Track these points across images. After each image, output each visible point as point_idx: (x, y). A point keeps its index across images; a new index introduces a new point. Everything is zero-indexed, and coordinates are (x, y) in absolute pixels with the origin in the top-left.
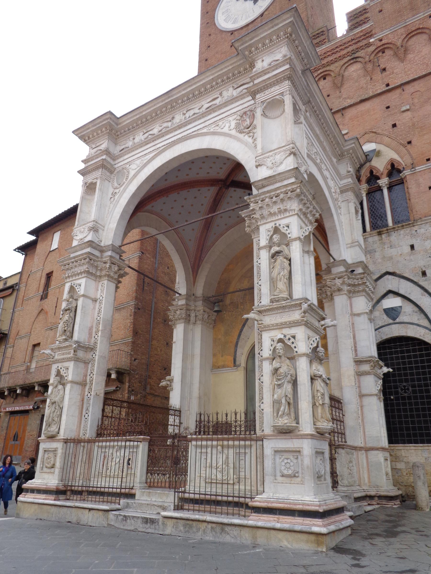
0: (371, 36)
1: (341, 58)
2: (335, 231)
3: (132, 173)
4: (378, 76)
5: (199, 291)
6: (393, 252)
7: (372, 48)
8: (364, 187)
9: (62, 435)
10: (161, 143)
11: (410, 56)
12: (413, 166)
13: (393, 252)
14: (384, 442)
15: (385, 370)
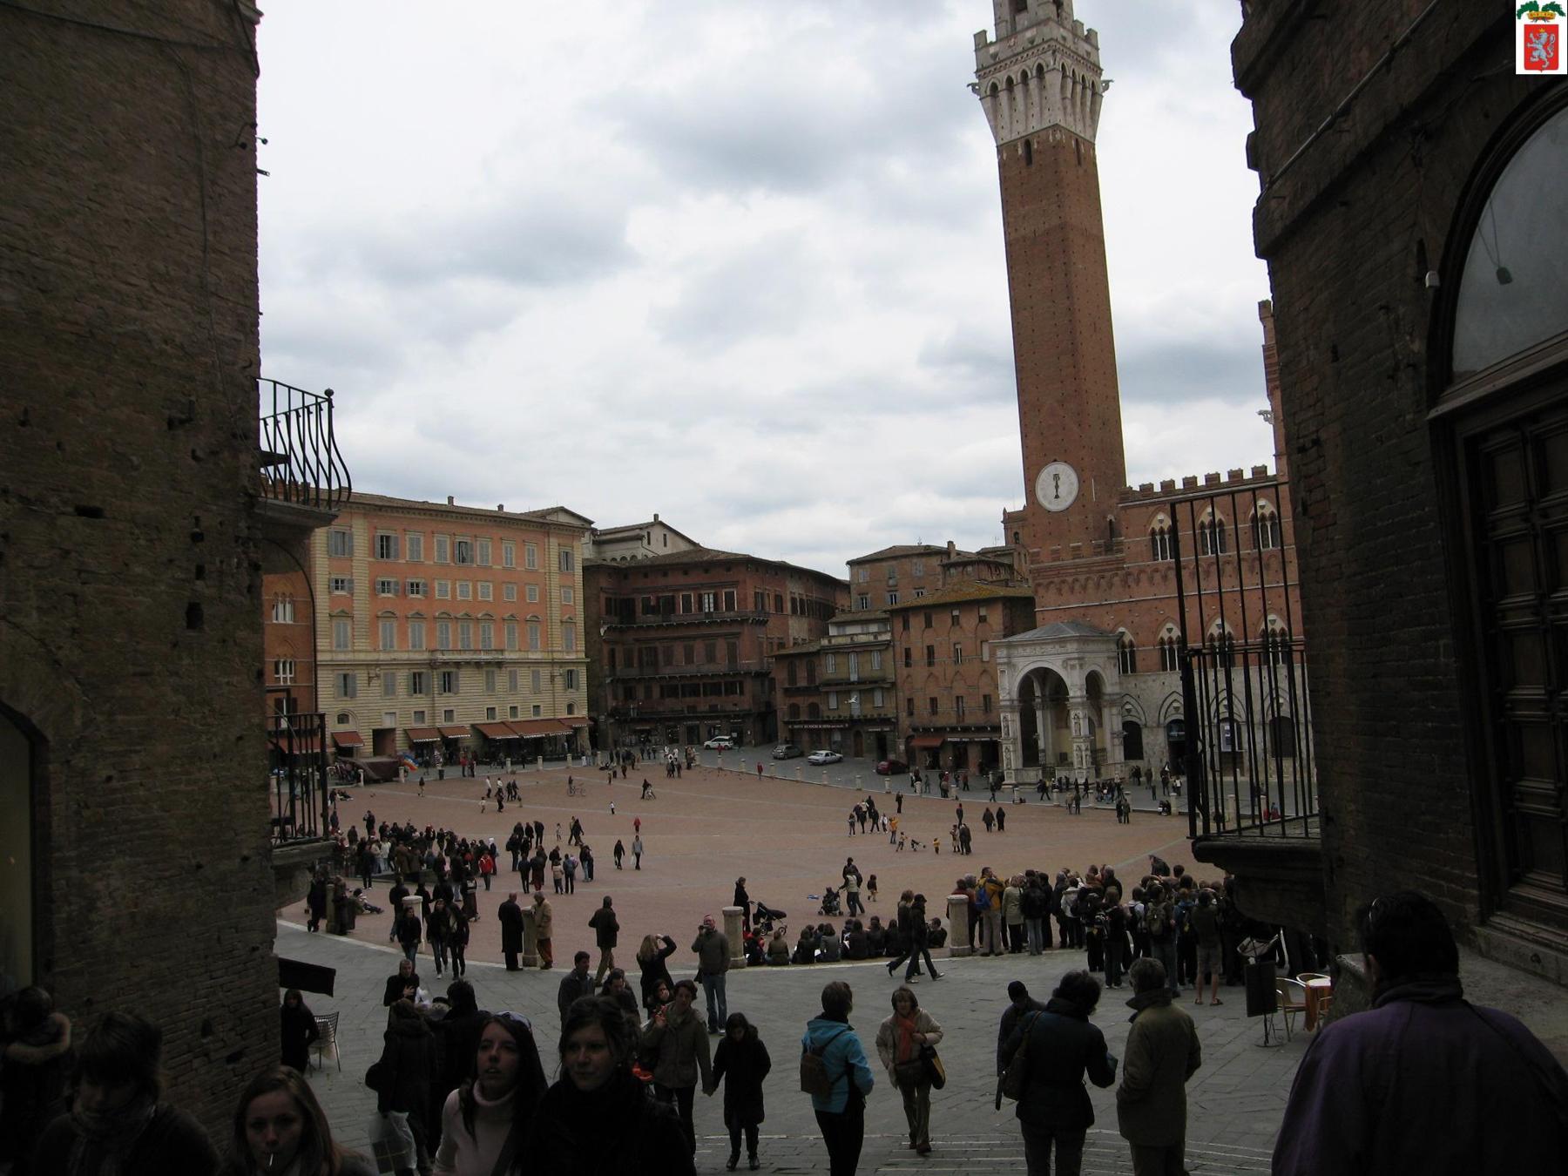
0: (1124, 563)
1: (1111, 570)
2: (1105, 684)
3: (1020, 668)
4: (1127, 589)
5: (1047, 693)
6: (1129, 686)
7: (1124, 572)
8: (1120, 650)
9: (1013, 768)
10: (1031, 659)
11: (1141, 584)
12: (1138, 647)
13: (1129, 686)
14: (1123, 760)
15: (1125, 733)
